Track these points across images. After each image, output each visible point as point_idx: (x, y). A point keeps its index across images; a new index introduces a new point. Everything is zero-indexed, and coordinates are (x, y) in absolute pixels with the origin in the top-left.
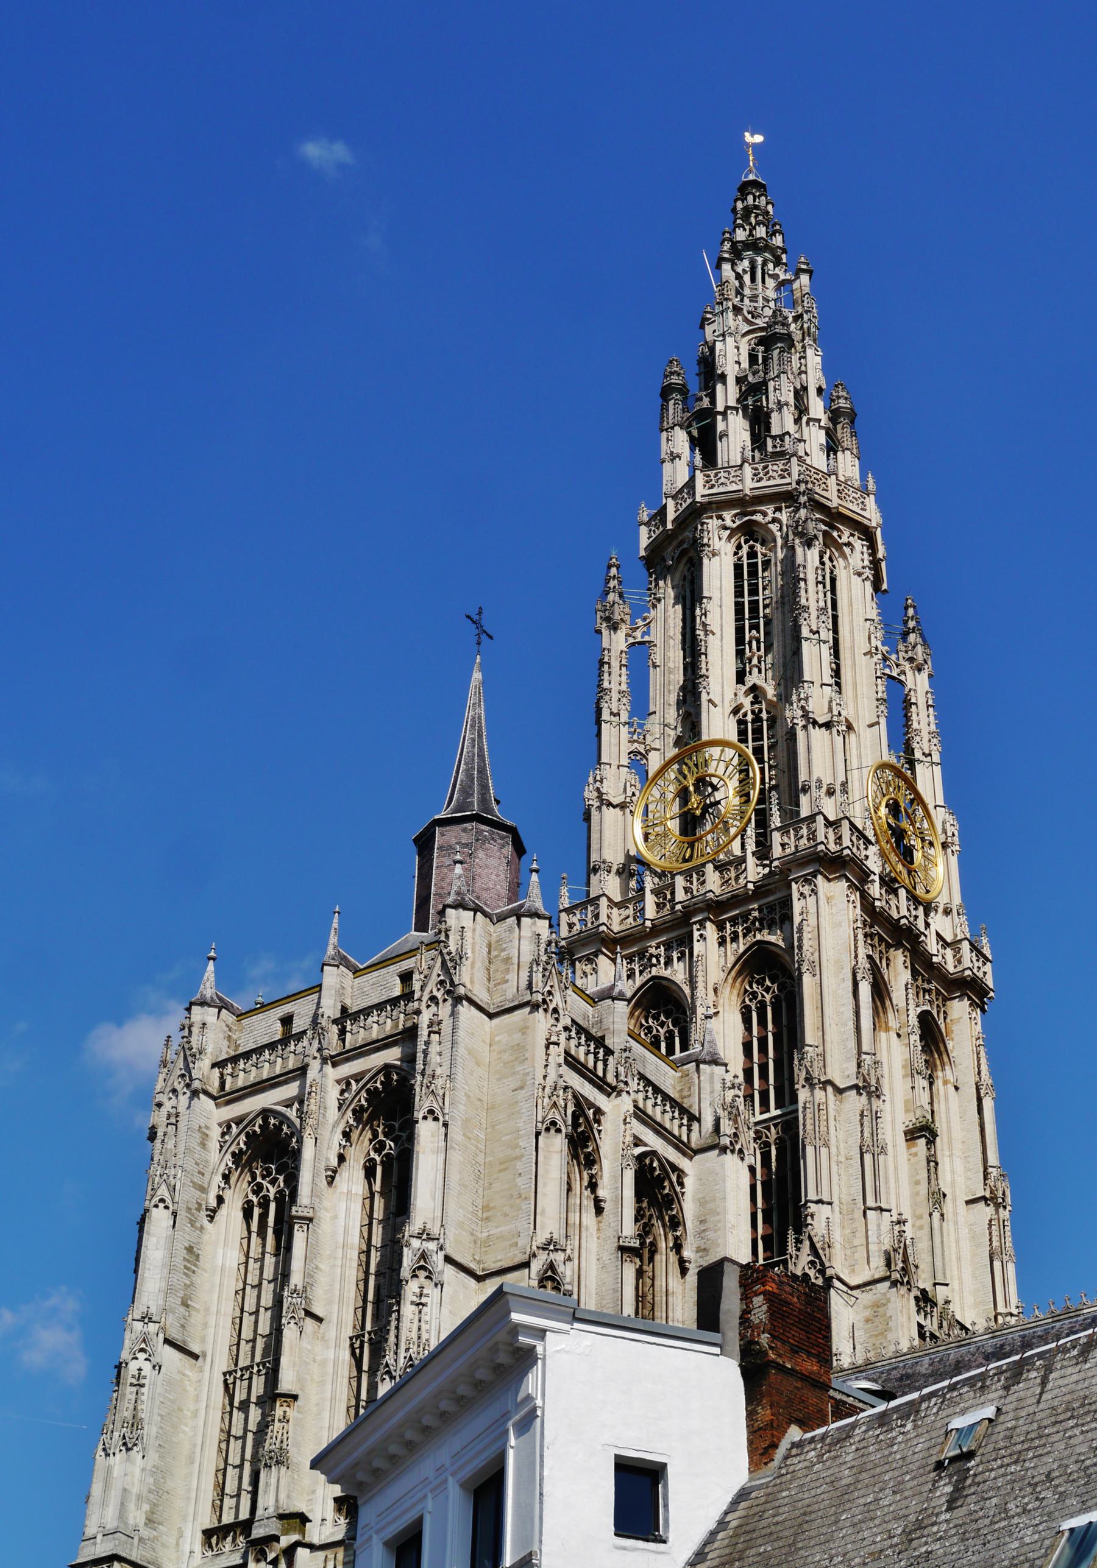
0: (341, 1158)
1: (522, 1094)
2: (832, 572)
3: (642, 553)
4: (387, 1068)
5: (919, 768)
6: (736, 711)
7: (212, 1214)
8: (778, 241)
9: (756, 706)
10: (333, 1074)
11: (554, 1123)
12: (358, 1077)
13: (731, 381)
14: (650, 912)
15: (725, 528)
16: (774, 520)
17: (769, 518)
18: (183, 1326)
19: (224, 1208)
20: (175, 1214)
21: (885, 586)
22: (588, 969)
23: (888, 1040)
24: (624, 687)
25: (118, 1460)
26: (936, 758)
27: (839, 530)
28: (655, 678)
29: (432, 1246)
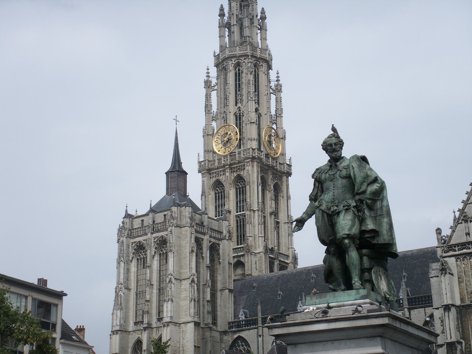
2: (258, 72)
5: (277, 118)
7: (131, 261)
9: (240, 112)
11: (193, 250)
15: (233, 63)
16: (244, 62)
17: (243, 61)
18: (127, 284)
19: (134, 260)
20: (124, 263)
23: (267, 192)
27: (259, 61)
29: (172, 277)
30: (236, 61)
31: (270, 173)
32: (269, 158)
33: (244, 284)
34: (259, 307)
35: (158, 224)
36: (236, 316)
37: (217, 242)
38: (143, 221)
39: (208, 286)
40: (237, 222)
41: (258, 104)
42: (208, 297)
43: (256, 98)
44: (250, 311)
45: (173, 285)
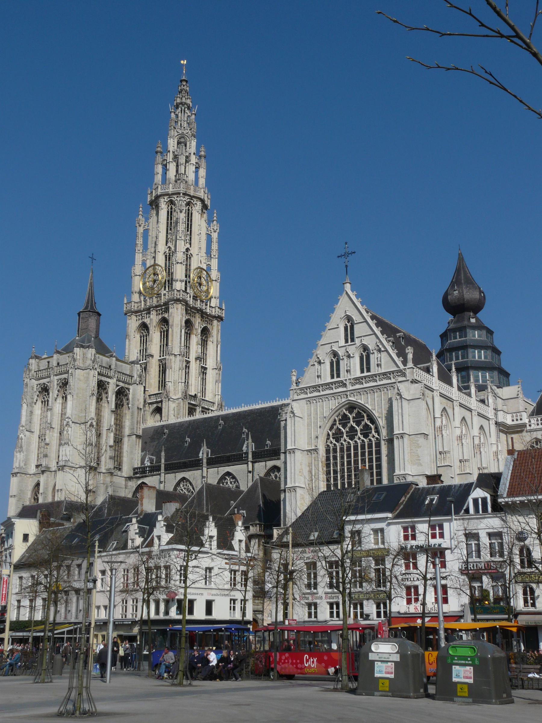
0: (57, 396)
1: (88, 388)
3: (148, 203)
4: (65, 379)
6: (165, 253)
7: (35, 403)
8: (189, 101)
10: (56, 378)
12: (60, 379)
13: (171, 152)
14: (143, 306)
19: (38, 403)
21: (209, 208)
22: (130, 318)
24: (141, 243)
25: (18, 454)
26: (217, 257)
28: (150, 238)
30: (169, 199)
31: (198, 316)
32: (197, 300)
33: (157, 431)
34: (163, 454)
35: (61, 365)
36: (142, 462)
37: (126, 386)
38: (48, 362)
39: (112, 431)
40: (160, 367)
41: (190, 244)
42: (111, 443)
43: (188, 238)
44: (156, 458)
45: (70, 429)
